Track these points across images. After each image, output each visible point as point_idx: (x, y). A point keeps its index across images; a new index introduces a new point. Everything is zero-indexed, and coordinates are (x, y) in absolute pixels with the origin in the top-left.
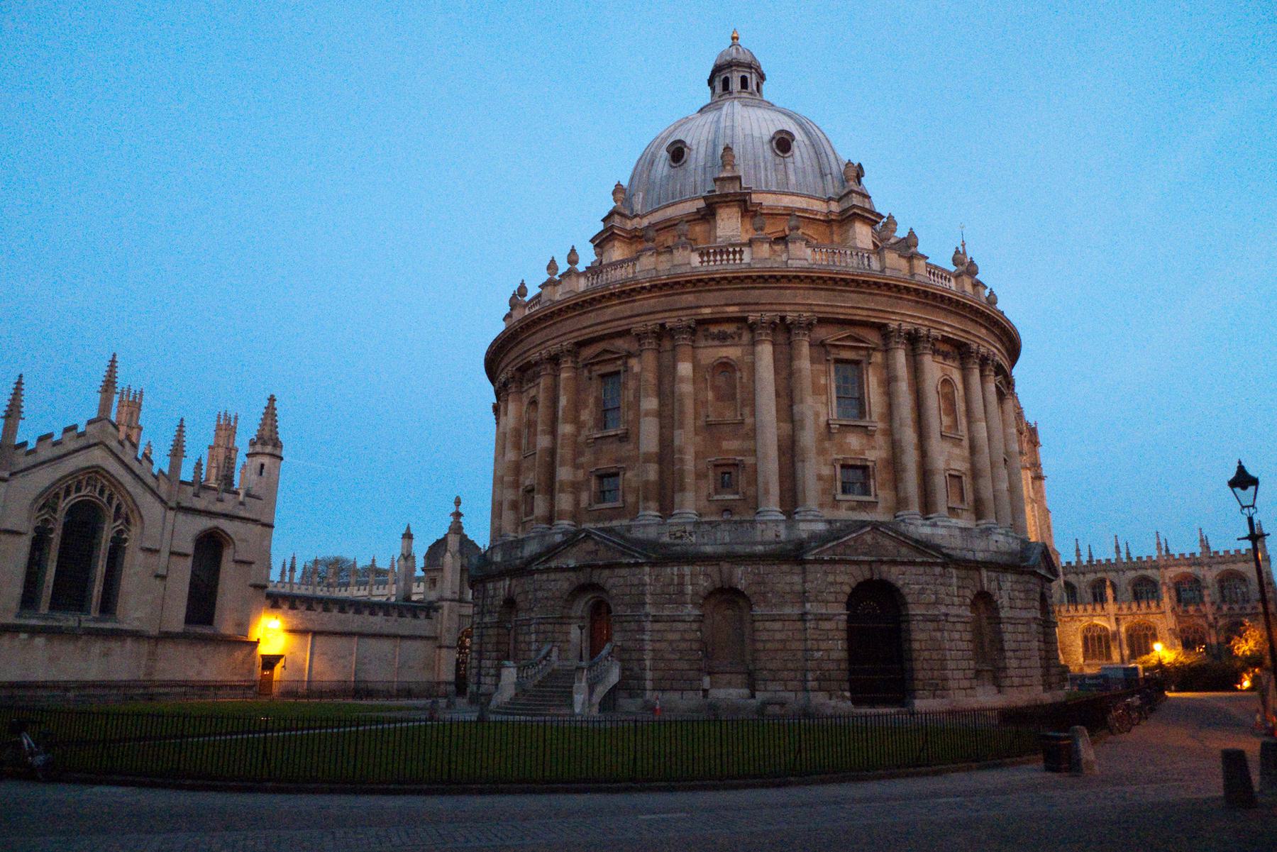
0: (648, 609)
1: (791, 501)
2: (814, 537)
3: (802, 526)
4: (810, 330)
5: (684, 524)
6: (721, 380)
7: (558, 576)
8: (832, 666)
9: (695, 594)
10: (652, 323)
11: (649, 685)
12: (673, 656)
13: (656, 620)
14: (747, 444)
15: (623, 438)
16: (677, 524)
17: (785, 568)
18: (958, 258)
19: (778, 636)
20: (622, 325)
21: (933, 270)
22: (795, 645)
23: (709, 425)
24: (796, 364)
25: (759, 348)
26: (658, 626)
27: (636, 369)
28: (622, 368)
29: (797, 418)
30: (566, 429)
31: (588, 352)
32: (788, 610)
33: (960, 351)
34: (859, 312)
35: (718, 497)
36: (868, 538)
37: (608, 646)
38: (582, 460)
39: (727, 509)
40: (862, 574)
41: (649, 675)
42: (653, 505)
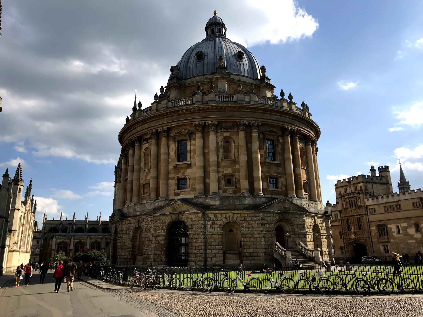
7: (272, 215)
15: (278, 165)
38: (263, 169)
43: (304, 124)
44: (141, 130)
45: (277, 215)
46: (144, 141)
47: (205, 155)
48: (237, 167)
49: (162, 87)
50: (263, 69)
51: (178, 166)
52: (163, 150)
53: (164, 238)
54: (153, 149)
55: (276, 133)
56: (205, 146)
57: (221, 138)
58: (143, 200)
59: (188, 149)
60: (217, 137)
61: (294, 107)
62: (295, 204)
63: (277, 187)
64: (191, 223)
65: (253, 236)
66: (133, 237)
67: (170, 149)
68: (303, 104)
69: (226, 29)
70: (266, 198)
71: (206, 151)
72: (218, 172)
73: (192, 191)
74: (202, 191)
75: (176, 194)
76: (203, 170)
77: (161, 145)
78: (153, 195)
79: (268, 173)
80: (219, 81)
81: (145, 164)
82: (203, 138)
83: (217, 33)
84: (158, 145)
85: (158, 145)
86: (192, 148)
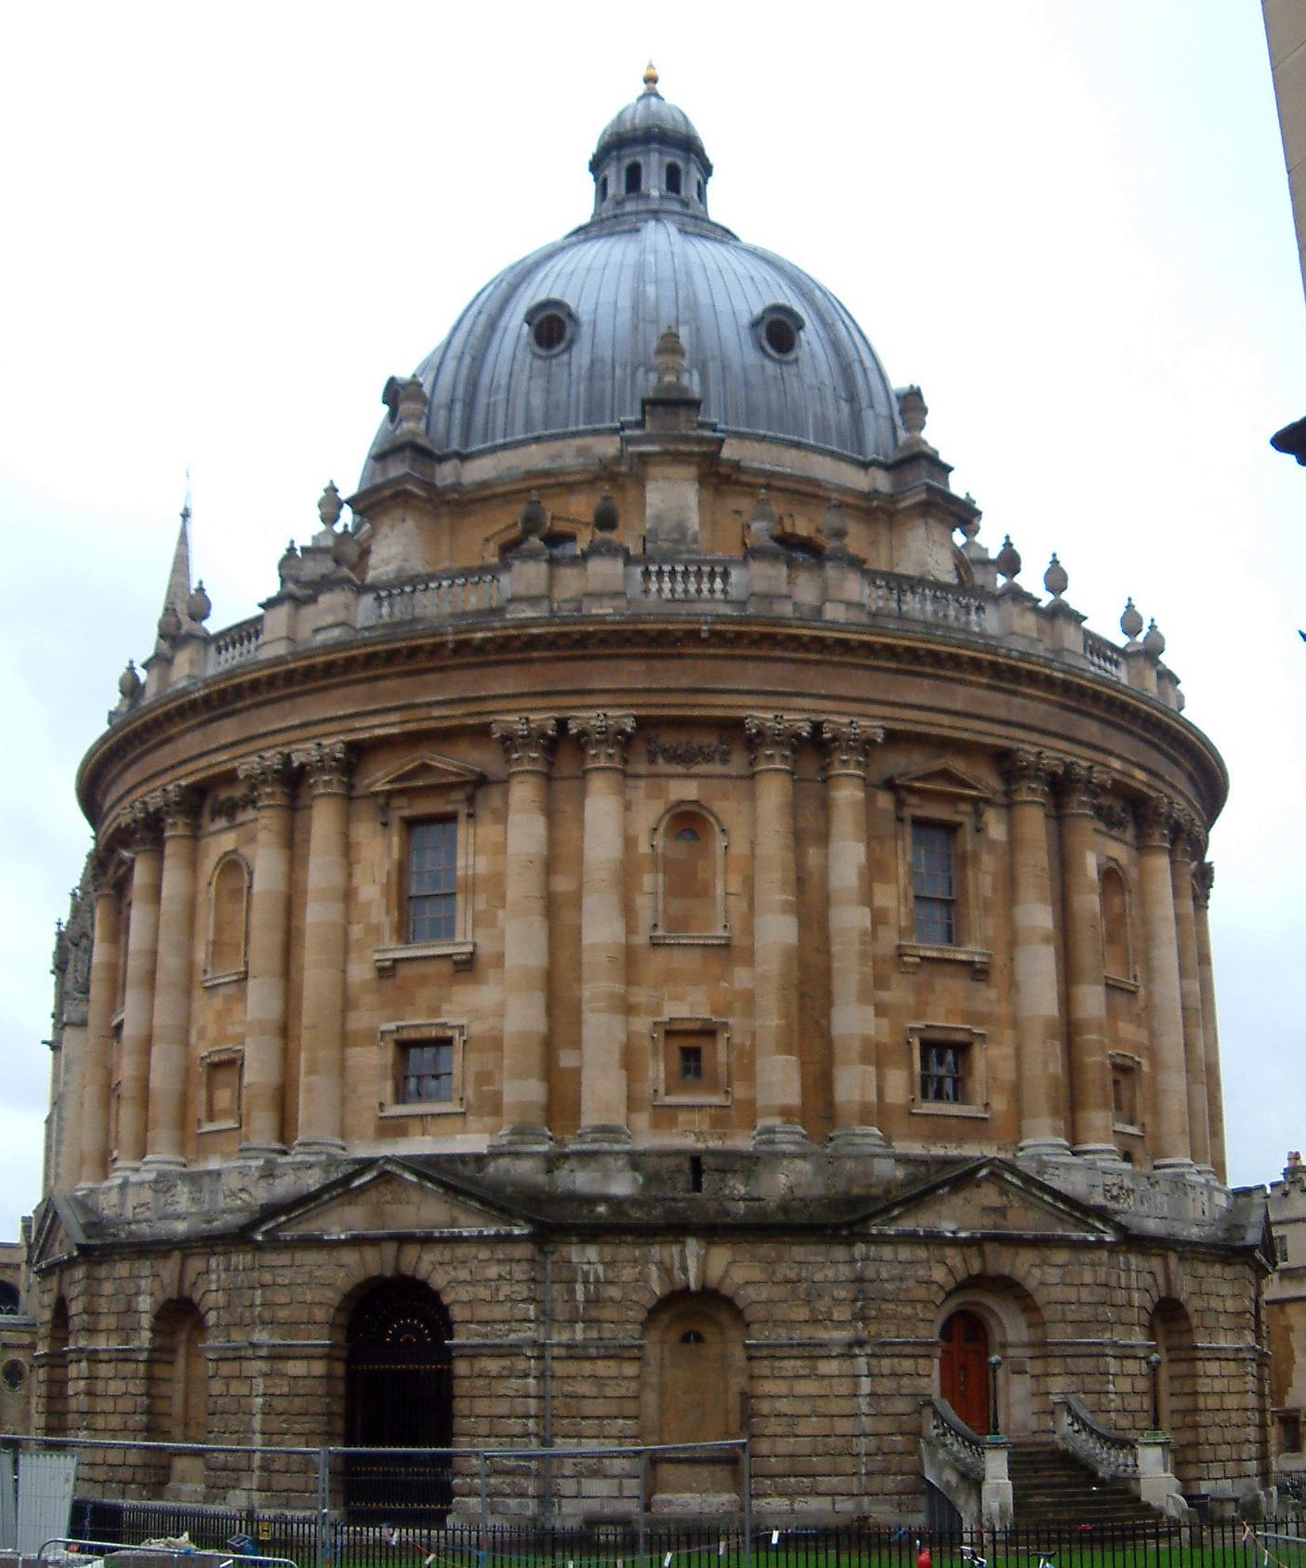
10: (1054, 754)
15: (978, 972)
20: (997, 736)
28: (968, 822)
38: (885, 996)
43: (1131, 733)
44: (201, 755)
45: (949, 1252)
46: (215, 814)
47: (557, 912)
48: (742, 977)
49: (332, 490)
50: (912, 404)
51: (404, 970)
52: (321, 870)
53: (319, 1368)
54: (266, 866)
55: (971, 787)
56: (558, 857)
57: (649, 812)
58: (202, 1152)
59: (460, 873)
60: (627, 807)
61: (1072, 640)
62: (1056, 1194)
63: (960, 1095)
64: (464, 1294)
65: (815, 1368)
66: (151, 1351)
67: (359, 871)
68: (1131, 622)
69: (707, 169)
70: (902, 1160)
71: (562, 884)
72: (629, 1009)
73: (480, 1113)
74: (536, 1117)
75: (392, 1128)
76: (539, 998)
77: (307, 841)
78: (262, 1127)
79: (919, 1015)
80: (654, 471)
81: (217, 947)
82: (550, 811)
83: (655, 193)
84: (293, 843)
85: (293, 843)
86: (483, 865)
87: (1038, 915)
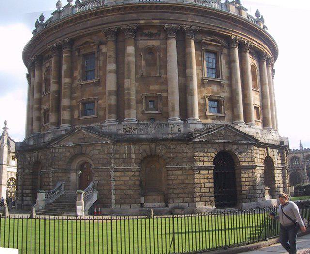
0: (113, 165)
1: (186, 113)
2: (197, 131)
3: (191, 126)
4: (195, 35)
5: (131, 125)
6: (149, 57)
8: (207, 190)
9: (136, 158)
10: (114, 27)
11: (113, 201)
12: (125, 188)
13: (116, 171)
14: (163, 87)
15: (98, 84)
16: (127, 125)
17: (183, 145)
18: (257, 14)
19: (180, 177)
21: (248, 16)
22: (187, 182)
23: (142, 77)
24: (187, 50)
25: (169, 41)
26: (117, 174)
27: (104, 50)
29: (188, 75)
30: (66, 80)
31: (78, 44)
32: (184, 166)
33: (259, 55)
34: (218, 29)
35: (147, 112)
36: (223, 132)
37: (91, 183)
38: (75, 95)
39: (152, 119)
40: (220, 149)
41: (113, 197)
42: (113, 115)
45: (70, 149)
87: (111, 67)
